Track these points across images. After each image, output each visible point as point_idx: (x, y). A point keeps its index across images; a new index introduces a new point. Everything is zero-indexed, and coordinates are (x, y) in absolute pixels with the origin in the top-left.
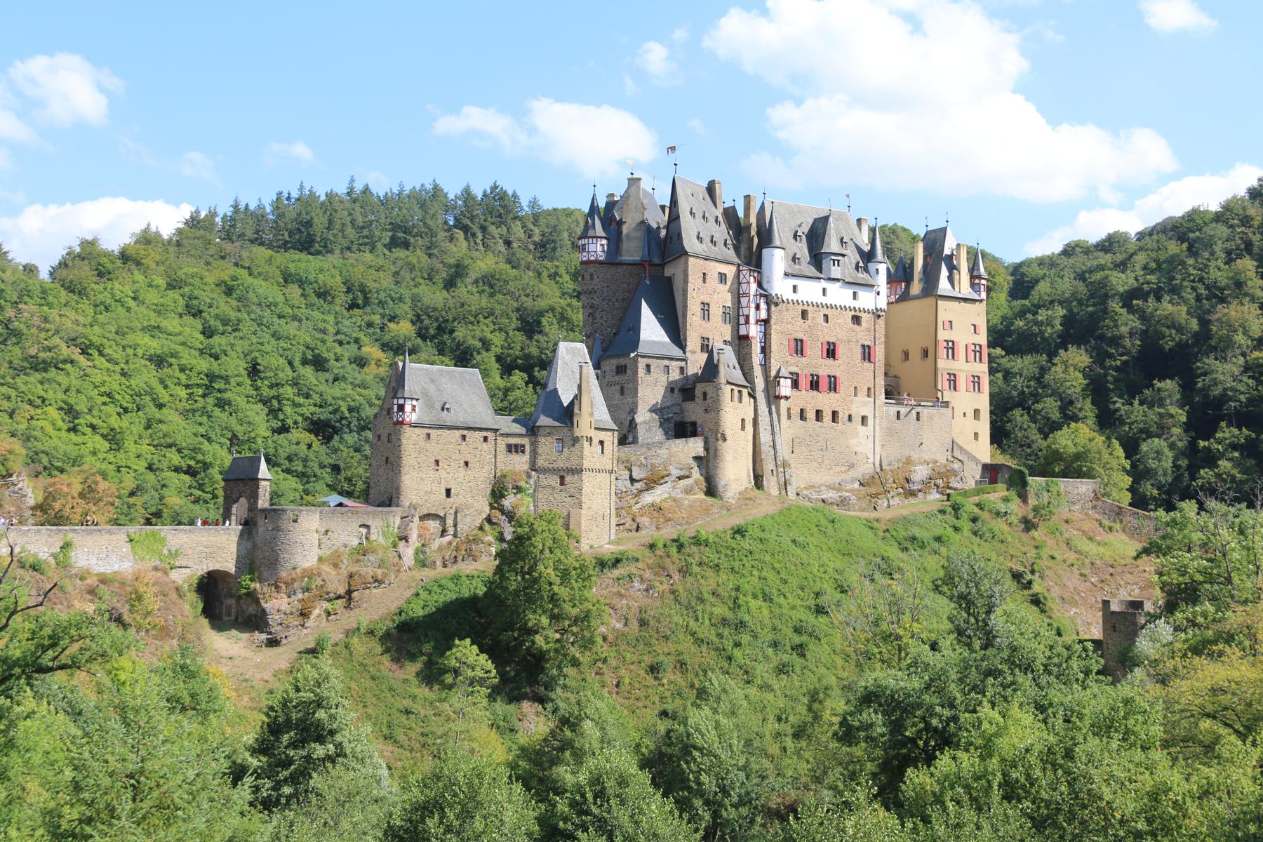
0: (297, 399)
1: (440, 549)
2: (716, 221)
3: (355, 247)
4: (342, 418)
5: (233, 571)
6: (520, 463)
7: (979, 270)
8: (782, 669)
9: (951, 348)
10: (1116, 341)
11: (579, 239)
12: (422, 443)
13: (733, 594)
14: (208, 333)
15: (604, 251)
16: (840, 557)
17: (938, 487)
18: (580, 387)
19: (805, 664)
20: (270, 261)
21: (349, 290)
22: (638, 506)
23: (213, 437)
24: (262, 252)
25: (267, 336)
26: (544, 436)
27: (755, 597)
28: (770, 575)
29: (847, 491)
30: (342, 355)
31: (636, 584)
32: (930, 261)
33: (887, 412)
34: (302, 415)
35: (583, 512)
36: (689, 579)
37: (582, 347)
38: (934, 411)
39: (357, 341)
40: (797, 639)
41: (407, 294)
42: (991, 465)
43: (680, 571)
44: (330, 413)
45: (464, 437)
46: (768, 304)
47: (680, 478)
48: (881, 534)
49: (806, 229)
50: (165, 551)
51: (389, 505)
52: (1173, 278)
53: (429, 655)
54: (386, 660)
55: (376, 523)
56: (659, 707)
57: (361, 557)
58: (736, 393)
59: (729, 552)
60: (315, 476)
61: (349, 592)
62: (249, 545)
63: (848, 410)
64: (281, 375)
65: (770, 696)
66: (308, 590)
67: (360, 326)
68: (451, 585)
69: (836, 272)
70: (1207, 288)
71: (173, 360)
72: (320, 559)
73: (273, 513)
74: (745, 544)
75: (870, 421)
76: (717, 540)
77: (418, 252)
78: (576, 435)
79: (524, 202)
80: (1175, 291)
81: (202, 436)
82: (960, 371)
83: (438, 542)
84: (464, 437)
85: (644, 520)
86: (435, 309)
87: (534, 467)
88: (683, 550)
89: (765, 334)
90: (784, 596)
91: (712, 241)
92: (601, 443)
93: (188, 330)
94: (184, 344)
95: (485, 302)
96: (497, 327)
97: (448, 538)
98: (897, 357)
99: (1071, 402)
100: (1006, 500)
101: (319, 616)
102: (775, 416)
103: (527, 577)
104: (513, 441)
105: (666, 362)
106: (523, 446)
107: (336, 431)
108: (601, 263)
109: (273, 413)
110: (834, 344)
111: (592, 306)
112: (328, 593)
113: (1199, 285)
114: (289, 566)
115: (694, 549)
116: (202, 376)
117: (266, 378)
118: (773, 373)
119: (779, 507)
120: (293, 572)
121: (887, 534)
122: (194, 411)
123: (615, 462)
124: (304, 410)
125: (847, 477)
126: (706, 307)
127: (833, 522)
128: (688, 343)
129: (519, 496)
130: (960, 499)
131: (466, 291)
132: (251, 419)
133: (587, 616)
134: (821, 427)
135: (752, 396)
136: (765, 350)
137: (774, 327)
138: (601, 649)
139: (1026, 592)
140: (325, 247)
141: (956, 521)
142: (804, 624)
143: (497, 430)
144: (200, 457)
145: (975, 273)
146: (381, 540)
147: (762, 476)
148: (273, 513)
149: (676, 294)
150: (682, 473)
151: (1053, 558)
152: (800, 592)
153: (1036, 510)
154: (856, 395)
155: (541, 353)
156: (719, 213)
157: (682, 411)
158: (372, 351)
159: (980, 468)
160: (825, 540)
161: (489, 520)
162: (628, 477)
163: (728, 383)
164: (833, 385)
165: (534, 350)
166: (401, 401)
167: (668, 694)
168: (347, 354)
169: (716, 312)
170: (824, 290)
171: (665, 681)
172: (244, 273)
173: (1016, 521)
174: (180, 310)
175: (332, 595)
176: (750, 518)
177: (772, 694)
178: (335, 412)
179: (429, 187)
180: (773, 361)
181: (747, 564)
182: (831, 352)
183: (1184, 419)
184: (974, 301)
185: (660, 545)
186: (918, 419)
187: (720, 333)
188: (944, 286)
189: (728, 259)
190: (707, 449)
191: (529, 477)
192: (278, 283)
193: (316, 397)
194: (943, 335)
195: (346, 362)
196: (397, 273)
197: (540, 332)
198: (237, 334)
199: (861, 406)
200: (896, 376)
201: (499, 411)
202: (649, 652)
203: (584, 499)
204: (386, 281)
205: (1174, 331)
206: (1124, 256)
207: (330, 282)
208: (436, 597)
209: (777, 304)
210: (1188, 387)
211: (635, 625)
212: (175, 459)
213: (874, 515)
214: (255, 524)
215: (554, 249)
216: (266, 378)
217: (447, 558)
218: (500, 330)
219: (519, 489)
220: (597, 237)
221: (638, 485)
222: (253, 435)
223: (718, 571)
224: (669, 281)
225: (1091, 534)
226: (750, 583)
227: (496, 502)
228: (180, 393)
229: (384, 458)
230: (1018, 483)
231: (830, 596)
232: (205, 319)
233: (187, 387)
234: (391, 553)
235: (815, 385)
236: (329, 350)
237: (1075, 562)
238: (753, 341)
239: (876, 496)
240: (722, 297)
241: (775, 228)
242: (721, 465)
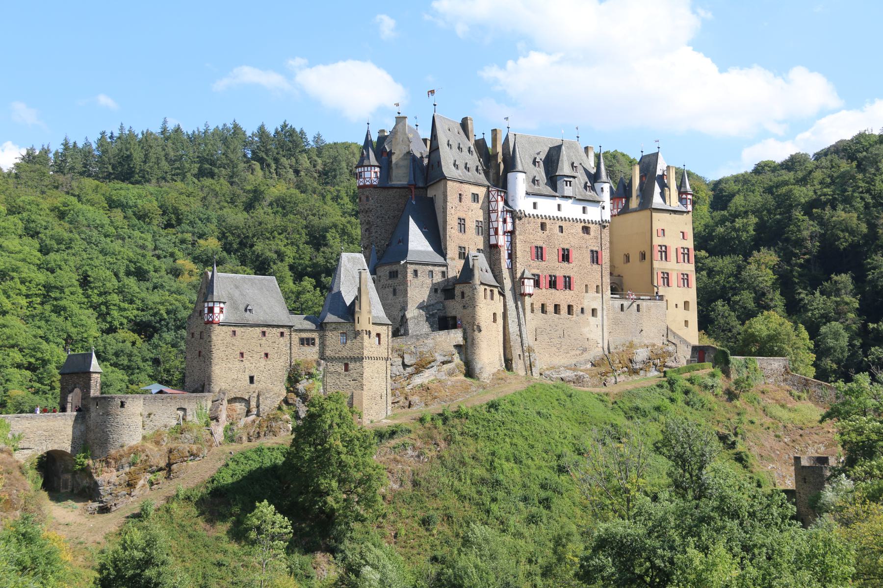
0: (122, 305)
1: (246, 426)
2: (469, 151)
3: (169, 177)
4: (161, 320)
5: (69, 450)
6: (311, 353)
7: (685, 187)
8: (532, 520)
9: (664, 251)
10: (799, 243)
11: (356, 167)
12: (229, 339)
13: (490, 458)
14: (45, 250)
15: (377, 177)
16: (577, 425)
17: (656, 365)
18: (359, 289)
19: (551, 514)
20: (96, 189)
21: (164, 213)
22: (410, 387)
23: (51, 338)
24: (89, 183)
25: (96, 252)
26: (331, 330)
27: (508, 460)
28: (520, 442)
29: (581, 371)
30: (160, 267)
31: (410, 452)
32: (645, 180)
33: (613, 305)
34: (127, 318)
35: (364, 393)
36: (453, 446)
37: (361, 256)
38: (651, 303)
39: (172, 255)
40: (543, 494)
41: (213, 215)
42: (699, 347)
43: (445, 440)
44: (151, 315)
45: (264, 333)
46: (513, 218)
47: (444, 363)
48: (610, 405)
49: (543, 156)
50: (10, 436)
51: (202, 391)
52: (845, 190)
53: (238, 516)
54: (201, 523)
55: (191, 406)
56: (430, 554)
57: (179, 435)
58: (488, 292)
59: (485, 423)
60: (138, 368)
62: (83, 428)
63: (581, 304)
64: (108, 285)
65: (521, 542)
66: (134, 464)
67: (174, 243)
68: (255, 456)
69: (568, 191)
70: (873, 198)
71: (14, 274)
72: (144, 438)
73: (103, 401)
74: (498, 416)
75: (599, 313)
76: (475, 413)
77: (222, 179)
78: (357, 329)
79: (310, 138)
80: (847, 201)
81: (41, 337)
82: (672, 270)
83: (244, 421)
84: (264, 333)
85: (415, 399)
86: (237, 228)
87: (322, 357)
88: (448, 423)
89: (511, 243)
90: (532, 458)
91: (466, 167)
92: (378, 335)
93: (27, 249)
94: (24, 260)
95: (279, 221)
96: (289, 242)
98: (620, 259)
99: (764, 294)
100: (713, 375)
101: (144, 486)
102: (520, 310)
103: (320, 447)
104: (305, 335)
105: (430, 268)
106: (313, 339)
107: (156, 330)
108: (375, 187)
109: (102, 316)
110: (568, 250)
112: (151, 466)
113: (867, 196)
114: (118, 444)
115: (457, 421)
116: (40, 287)
117: (96, 288)
118: (519, 275)
119: (526, 385)
120: (121, 449)
121: (615, 405)
122: (33, 316)
123: (390, 351)
124: (127, 314)
125: (581, 359)
126: (463, 221)
127: (570, 396)
128: (448, 252)
129: (310, 381)
130: (675, 376)
131: (262, 212)
132: (84, 322)
133: (369, 478)
134: (559, 319)
135: (502, 294)
136: (512, 256)
138: (382, 506)
139: (731, 451)
140: (143, 177)
141: (671, 394)
142: (548, 482)
143: (292, 327)
144: (39, 355)
145: (683, 190)
146: (196, 420)
147: (511, 360)
148: (103, 401)
149: (437, 211)
150: (445, 359)
151: (752, 422)
152: (544, 455)
153: (737, 383)
154: (587, 292)
155: (327, 262)
156: (471, 144)
157: (444, 307)
158: (185, 263)
159: (690, 349)
160: (563, 411)
161: (286, 401)
162: (400, 363)
163: (482, 284)
164: (568, 284)
165: (320, 260)
166: (211, 305)
167: (437, 542)
168: (164, 267)
169: (471, 225)
170: (559, 206)
171: (435, 532)
172: (74, 200)
173: (721, 393)
174: (20, 232)
175: (154, 468)
176: (501, 395)
177: (524, 540)
178: (155, 315)
179: (230, 125)
180: (518, 265)
181: (500, 433)
182: (566, 257)
183: (857, 305)
184: (682, 212)
185: (428, 419)
186: (638, 310)
187: (474, 243)
188: (657, 200)
189: (480, 182)
190: (465, 338)
191: (319, 364)
192: (104, 208)
193: (138, 302)
194: (657, 241)
195: (163, 273)
196: (205, 198)
197: (326, 245)
198: (70, 251)
199: (592, 300)
200: (619, 276)
201: (292, 311)
202: (421, 508)
203: (364, 382)
204: (196, 205)
205: (847, 234)
206: (804, 173)
207: (148, 206)
208: (242, 467)
209: (520, 219)
210: (859, 280)
211: (409, 485)
212: (18, 357)
213: (604, 390)
214: (88, 410)
215: (335, 177)
216: (96, 288)
217: (251, 434)
218: (292, 244)
219: (310, 375)
220: (371, 166)
221: (409, 370)
222: (85, 335)
223: (476, 439)
224: (432, 201)
225: (783, 402)
226: (504, 449)
227: (291, 386)
228: (21, 301)
229: (197, 352)
230: (722, 362)
231: (570, 457)
232: (42, 239)
233: (27, 296)
234: (204, 432)
235: (553, 284)
236: (149, 263)
237: (771, 426)
238: (502, 249)
239: (605, 374)
240: (475, 214)
241: (518, 156)
242: (477, 352)
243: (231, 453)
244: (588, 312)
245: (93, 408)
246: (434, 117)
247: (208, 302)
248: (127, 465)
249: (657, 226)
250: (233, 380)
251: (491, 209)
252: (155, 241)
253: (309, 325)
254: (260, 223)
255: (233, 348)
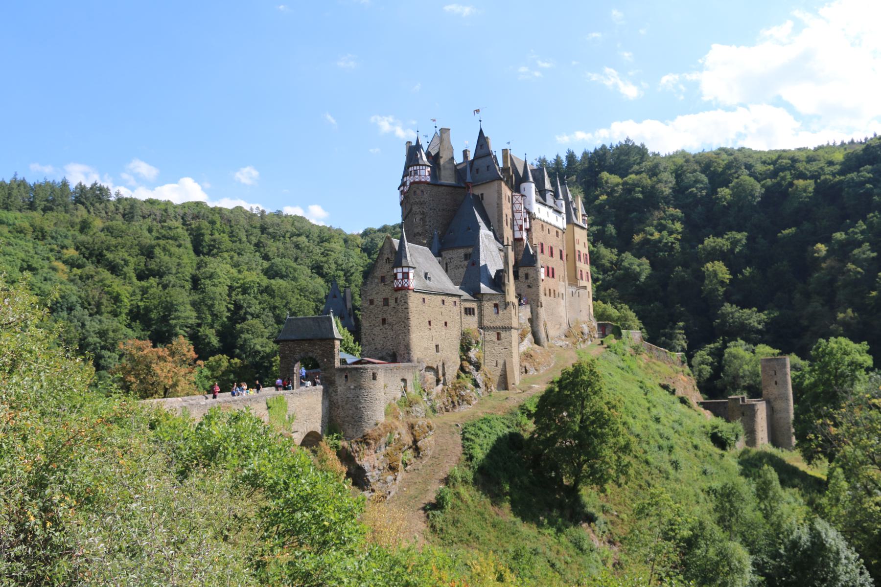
1: (438, 397)
5: (320, 432)
6: (471, 322)
9: (579, 256)
39: (48, 258)
41: (69, 234)
45: (443, 301)
50: (287, 417)
57: (408, 409)
61: (415, 441)
66: (388, 444)
79: (113, 192)
84: (443, 301)
86: (88, 243)
87: (481, 326)
97: (440, 386)
104: (468, 305)
108: (428, 183)
111: (423, 213)
114: (372, 422)
129: (477, 349)
137: (534, 234)
148: (354, 372)
158: (59, 265)
161: (462, 369)
165: (153, 266)
166: (406, 270)
190: (532, 313)
191: (481, 334)
193: (37, 289)
209: (534, 219)
215: (133, 217)
217: (447, 404)
236: (36, 262)
243: (457, 425)
244: (561, 295)
245: (340, 381)
246: (481, 131)
247: (403, 267)
248: (383, 446)
249: (577, 237)
250: (426, 349)
251: (514, 209)
252: (35, 248)
253: (466, 295)
254: (102, 242)
255: (424, 315)
